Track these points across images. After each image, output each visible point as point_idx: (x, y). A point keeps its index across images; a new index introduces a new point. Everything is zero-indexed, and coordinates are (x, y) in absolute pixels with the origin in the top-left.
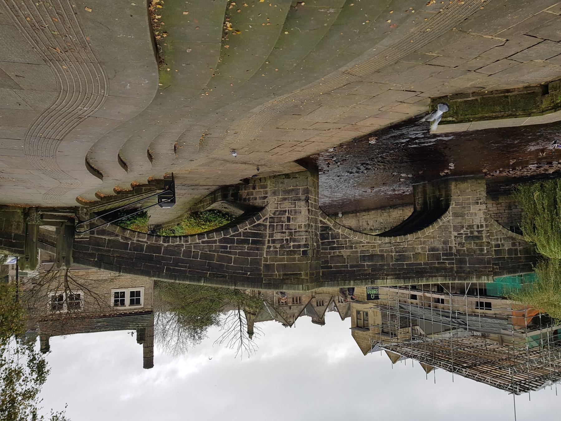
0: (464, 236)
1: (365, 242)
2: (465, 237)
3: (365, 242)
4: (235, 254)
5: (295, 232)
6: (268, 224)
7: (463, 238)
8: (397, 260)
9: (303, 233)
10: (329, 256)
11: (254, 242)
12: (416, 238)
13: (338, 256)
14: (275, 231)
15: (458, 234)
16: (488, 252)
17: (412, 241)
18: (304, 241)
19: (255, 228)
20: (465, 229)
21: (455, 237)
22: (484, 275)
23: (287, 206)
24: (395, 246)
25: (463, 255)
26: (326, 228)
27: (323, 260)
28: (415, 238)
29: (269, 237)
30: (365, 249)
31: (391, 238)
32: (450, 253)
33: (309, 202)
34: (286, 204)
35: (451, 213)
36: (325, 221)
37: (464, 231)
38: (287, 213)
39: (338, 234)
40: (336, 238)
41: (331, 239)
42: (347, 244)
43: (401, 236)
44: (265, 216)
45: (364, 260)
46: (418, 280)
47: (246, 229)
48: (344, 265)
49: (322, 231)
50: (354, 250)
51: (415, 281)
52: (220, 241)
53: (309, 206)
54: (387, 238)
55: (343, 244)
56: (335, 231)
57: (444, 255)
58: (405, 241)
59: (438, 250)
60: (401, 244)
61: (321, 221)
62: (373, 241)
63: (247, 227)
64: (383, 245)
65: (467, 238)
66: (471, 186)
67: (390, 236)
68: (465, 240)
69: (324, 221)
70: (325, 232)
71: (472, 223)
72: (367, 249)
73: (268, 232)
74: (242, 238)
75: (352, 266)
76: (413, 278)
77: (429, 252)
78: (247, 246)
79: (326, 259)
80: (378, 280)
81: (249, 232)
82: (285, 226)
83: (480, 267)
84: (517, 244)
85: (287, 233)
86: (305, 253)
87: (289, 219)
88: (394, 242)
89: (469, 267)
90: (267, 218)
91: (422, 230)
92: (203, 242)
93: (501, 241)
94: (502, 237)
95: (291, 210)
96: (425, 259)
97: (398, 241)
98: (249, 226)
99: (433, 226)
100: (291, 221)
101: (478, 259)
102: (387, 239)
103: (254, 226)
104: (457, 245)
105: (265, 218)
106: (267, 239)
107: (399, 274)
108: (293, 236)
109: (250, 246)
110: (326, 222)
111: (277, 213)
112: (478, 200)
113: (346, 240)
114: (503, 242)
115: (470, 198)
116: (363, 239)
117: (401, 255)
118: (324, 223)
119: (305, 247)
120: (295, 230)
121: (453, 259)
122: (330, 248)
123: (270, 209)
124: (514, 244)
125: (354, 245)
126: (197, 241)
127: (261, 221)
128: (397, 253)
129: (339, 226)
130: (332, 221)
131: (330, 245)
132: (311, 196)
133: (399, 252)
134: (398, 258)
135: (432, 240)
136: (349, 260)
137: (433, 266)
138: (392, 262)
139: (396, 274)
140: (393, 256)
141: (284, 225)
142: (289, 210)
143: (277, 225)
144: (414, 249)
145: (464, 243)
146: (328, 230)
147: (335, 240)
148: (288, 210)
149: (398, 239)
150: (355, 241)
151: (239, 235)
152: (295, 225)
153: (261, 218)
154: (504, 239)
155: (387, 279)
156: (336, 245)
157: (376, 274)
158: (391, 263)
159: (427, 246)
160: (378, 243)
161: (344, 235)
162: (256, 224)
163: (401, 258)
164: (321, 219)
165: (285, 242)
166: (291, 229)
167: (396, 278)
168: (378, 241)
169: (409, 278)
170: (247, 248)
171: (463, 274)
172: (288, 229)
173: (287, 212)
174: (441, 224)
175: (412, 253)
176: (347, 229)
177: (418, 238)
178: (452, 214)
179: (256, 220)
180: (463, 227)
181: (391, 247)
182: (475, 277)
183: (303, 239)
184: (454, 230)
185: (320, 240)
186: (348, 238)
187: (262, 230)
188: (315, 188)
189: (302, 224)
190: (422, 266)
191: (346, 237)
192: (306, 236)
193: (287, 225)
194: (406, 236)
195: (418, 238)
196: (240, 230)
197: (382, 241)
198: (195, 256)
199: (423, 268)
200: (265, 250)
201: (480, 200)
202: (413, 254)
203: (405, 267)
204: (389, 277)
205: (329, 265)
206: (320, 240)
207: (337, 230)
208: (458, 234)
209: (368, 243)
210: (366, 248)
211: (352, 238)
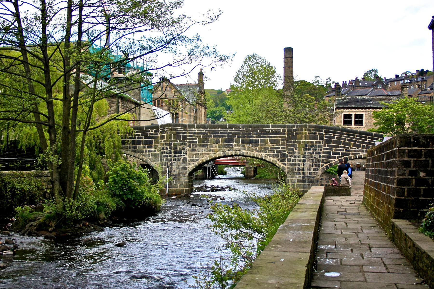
4: (341, 147)
6: (321, 164)
10: (280, 144)
11: (330, 153)
12: (216, 153)
28: (217, 154)
35: (188, 170)
36: (282, 165)
40: (276, 155)
45: (256, 140)
47: (334, 160)
49: (285, 159)
52: (349, 154)
57: (196, 142)
59: (200, 146)
73: (321, 159)
84: (131, 148)
90: (322, 167)
92: (359, 154)
103: (329, 162)
111: (317, 169)
114: (144, 150)
118: (283, 164)
124: (135, 148)
125: (263, 150)
126: (362, 154)
127: (325, 165)
134: (231, 141)
136: (267, 141)
147: (276, 153)
151: (338, 157)
154: (143, 152)
156: (276, 150)
159: (208, 148)
177: (215, 153)
186: (266, 154)
191: (268, 155)
198: (363, 147)
209: (252, 151)
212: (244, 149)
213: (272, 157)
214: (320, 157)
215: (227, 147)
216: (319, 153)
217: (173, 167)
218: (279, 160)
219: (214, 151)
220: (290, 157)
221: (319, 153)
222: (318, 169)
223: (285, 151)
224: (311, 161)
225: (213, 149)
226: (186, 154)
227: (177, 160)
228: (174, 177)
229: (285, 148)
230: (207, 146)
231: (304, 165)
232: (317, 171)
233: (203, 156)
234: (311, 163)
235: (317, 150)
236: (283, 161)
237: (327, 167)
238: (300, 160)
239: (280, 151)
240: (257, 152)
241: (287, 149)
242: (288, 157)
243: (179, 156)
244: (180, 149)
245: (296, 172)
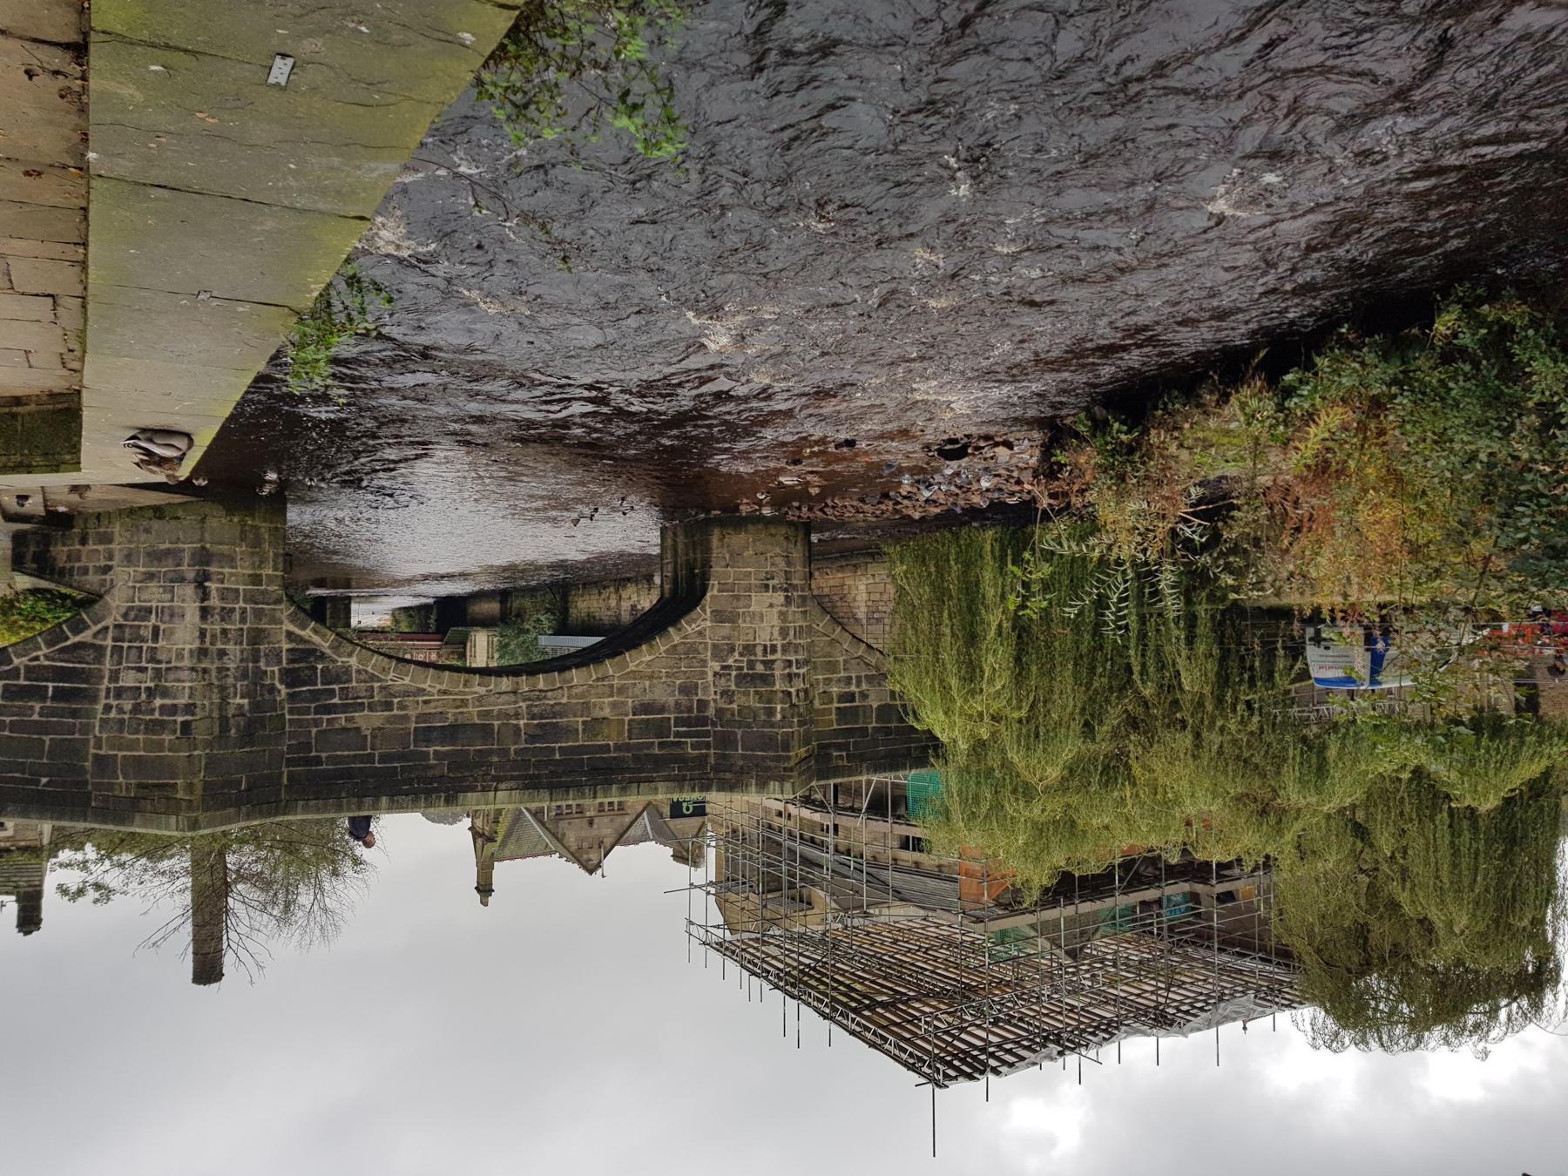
0: (734, 673)
1: (435, 691)
6: (109, 642)
8: (532, 738)
9: (185, 674)
10: (314, 730)
11: (60, 695)
13: (344, 729)
14: (125, 665)
15: (724, 668)
16: (784, 717)
19: (66, 656)
20: (736, 654)
22: (775, 780)
23: (154, 595)
25: (729, 723)
26: (305, 652)
27: (293, 742)
28: (594, 677)
29: (111, 680)
31: (519, 679)
32: (697, 718)
36: (306, 633)
37: (736, 661)
38: (153, 616)
39: (347, 670)
40: (337, 680)
41: (323, 684)
42: (372, 697)
43: (550, 675)
44: (99, 622)
45: (428, 742)
46: (595, 793)
47: (37, 658)
49: (291, 661)
50: (395, 712)
51: (583, 794)
54: (505, 679)
55: (359, 697)
56: (334, 661)
57: (679, 722)
60: (549, 694)
61: (289, 634)
62: (461, 688)
63: (39, 653)
65: (741, 678)
66: (754, 541)
68: (737, 686)
72: (439, 710)
73: (108, 665)
74: (22, 682)
76: (579, 786)
77: (634, 714)
78: (38, 706)
79: (302, 739)
80: (469, 794)
81: (45, 667)
83: (766, 757)
85: (150, 671)
89: (744, 757)
90: (106, 628)
91: (618, 658)
95: (163, 607)
96: (620, 733)
97: (541, 686)
98: (45, 650)
99: (651, 646)
101: (763, 735)
102: (506, 683)
103: (61, 650)
104: (718, 697)
105: (99, 626)
106: (103, 687)
107: (538, 777)
109: (48, 704)
110: (307, 638)
113: (372, 687)
116: (429, 683)
118: (301, 640)
122: (316, 708)
123: (117, 603)
125: (396, 700)
127: (86, 636)
128: (533, 719)
129: (350, 647)
130: (329, 633)
131: (318, 700)
134: (538, 732)
135: (647, 683)
137: (646, 751)
139: (525, 777)
143: (129, 647)
144: (586, 707)
146: (312, 659)
147: (336, 687)
149: (541, 681)
150: (402, 688)
153: (88, 627)
155: (496, 790)
156: (336, 700)
157: (464, 778)
158: (513, 748)
161: (366, 672)
162: (69, 643)
163: (547, 729)
164: (292, 628)
167: (526, 787)
168: (477, 689)
169: (566, 787)
170: (37, 709)
171: (728, 775)
174: (677, 639)
175: (580, 719)
176: (376, 656)
178: (712, 612)
179: (69, 634)
180: (732, 650)
181: (516, 702)
182: (754, 782)
183: (184, 688)
184: (715, 656)
186: (379, 680)
187: (88, 659)
190: (609, 752)
191: (373, 678)
192: (191, 681)
194: (567, 674)
195: (603, 679)
196: (16, 661)
197: (492, 687)
199: (615, 758)
200: (99, 716)
202: (584, 722)
203: (557, 757)
204: (503, 786)
208: (724, 668)
209: (445, 693)
212: (480, 699)
213: (354, 668)
214: (115, 676)
215: (552, 706)
216: (119, 693)
217: (776, 622)
218: (323, 657)
219: (607, 690)
220: (269, 669)
221: (119, 693)
222: (125, 616)
223: (292, 697)
224: (162, 656)
225: (611, 695)
226: (715, 674)
227: (759, 650)
228: (771, 583)
229: (291, 711)
230: (634, 707)
231: (203, 634)
232: (130, 609)
233: (649, 664)
234: (161, 643)
235: (128, 705)
236: (302, 651)
237: (78, 627)
238: (220, 659)
239: (315, 695)
240: (421, 691)
241: (283, 708)
242: (276, 669)
243: (751, 665)
244: (747, 694)
245: (242, 604)
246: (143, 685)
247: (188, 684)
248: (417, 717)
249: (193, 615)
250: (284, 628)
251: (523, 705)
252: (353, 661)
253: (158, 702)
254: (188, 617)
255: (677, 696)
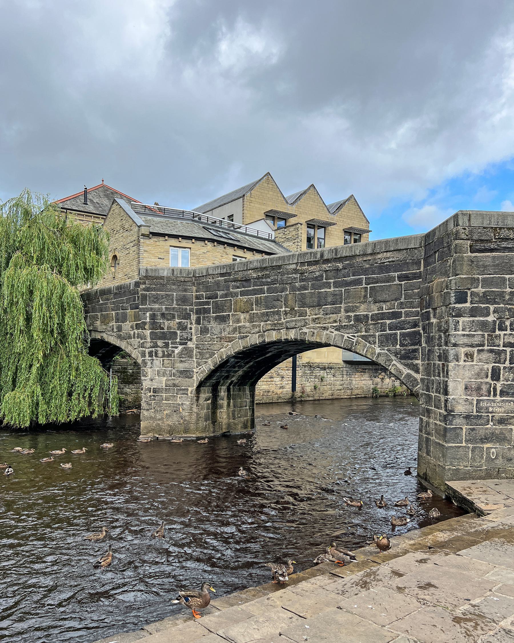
0: (178, 340)
1: (330, 329)
2: (177, 339)
3: (330, 329)
5: (483, 345)
7: (178, 337)
10: (402, 300)
12: (247, 337)
15: (186, 344)
17: (252, 332)
18: (460, 323)
21: (191, 340)
24: (280, 324)
30: (331, 315)
32: (200, 313)
33: (446, 410)
34: (499, 410)
37: (176, 348)
38: (499, 389)
39: (382, 345)
48: (372, 283)
53: (446, 401)
56: (389, 350)
57: (207, 311)
58: (264, 332)
59: (216, 318)
60: (269, 328)
61: (417, 371)
62: (315, 331)
64: (299, 324)
67: (286, 340)
69: (409, 371)
70: (410, 348)
71: (165, 361)
72: (328, 316)
75: (358, 282)
77: (229, 315)
82: (505, 361)
84: (115, 330)
85: (501, 343)
86: (461, 298)
87: (496, 375)
88: (281, 331)
93: (134, 333)
94: (133, 339)
95: (489, 396)
97: (274, 332)
100: (490, 371)
104: (189, 326)
108: (486, 336)
112: (154, 396)
115: (166, 400)
117: (272, 308)
119: (460, 309)
120: (482, 350)
121: (197, 304)
124: (119, 329)
125: (352, 323)
132: (438, 422)
133: (273, 312)
138: (287, 294)
140: (284, 306)
141: (507, 362)
142: (495, 395)
144: (251, 320)
145: (178, 329)
148: (495, 395)
149: (273, 336)
152: (480, 360)
154: (130, 337)
156: (388, 322)
159: (231, 324)
160: (308, 328)
161: (369, 342)
165: (508, 323)
166: (491, 351)
172: (499, 353)
173: (498, 392)
175: (255, 312)
181: (287, 322)
185: (422, 332)
188: (427, 440)
189: (465, 361)
193: (499, 362)
201: (150, 396)
205: (403, 283)
206: (422, 332)
207: (383, 351)
209: (325, 328)
210: (330, 318)
211: (354, 336)
213: (377, 345)
215: (268, 320)
218: (396, 354)
236: (409, 358)
244: (169, 328)
246: (508, 332)
247: (461, 333)
248: (340, 311)
249: (456, 389)
250: (420, 375)
251: (283, 320)
252: (378, 350)
253: (491, 318)
254: (461, 388)
255: (209, 326)
